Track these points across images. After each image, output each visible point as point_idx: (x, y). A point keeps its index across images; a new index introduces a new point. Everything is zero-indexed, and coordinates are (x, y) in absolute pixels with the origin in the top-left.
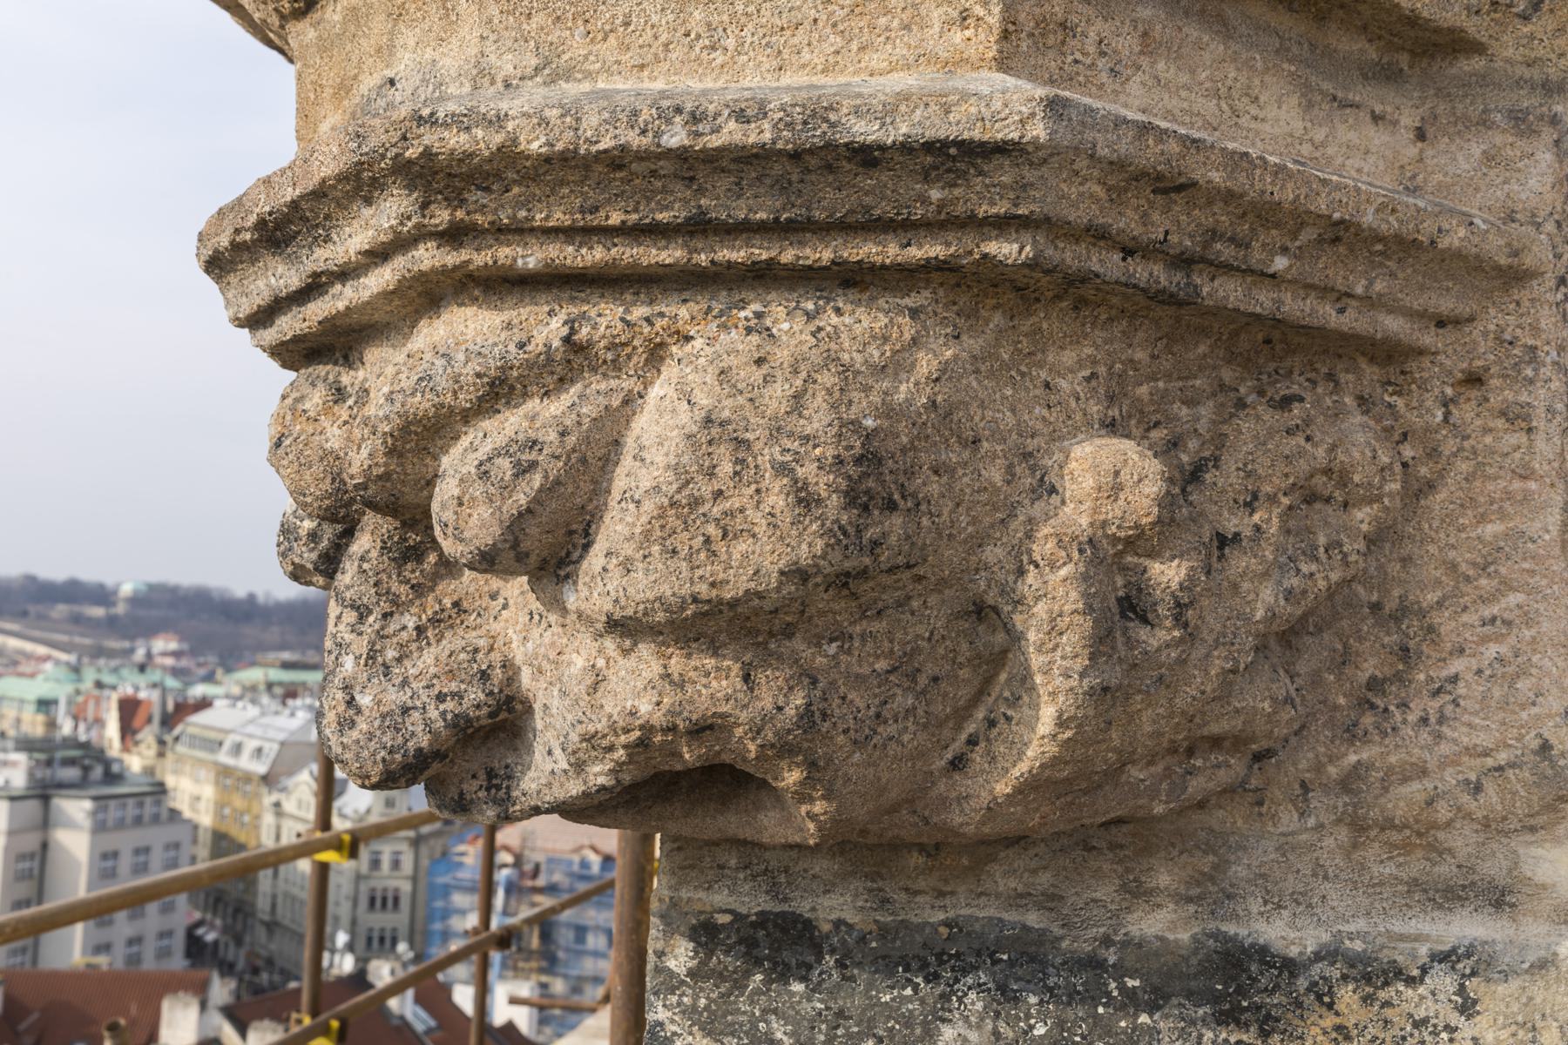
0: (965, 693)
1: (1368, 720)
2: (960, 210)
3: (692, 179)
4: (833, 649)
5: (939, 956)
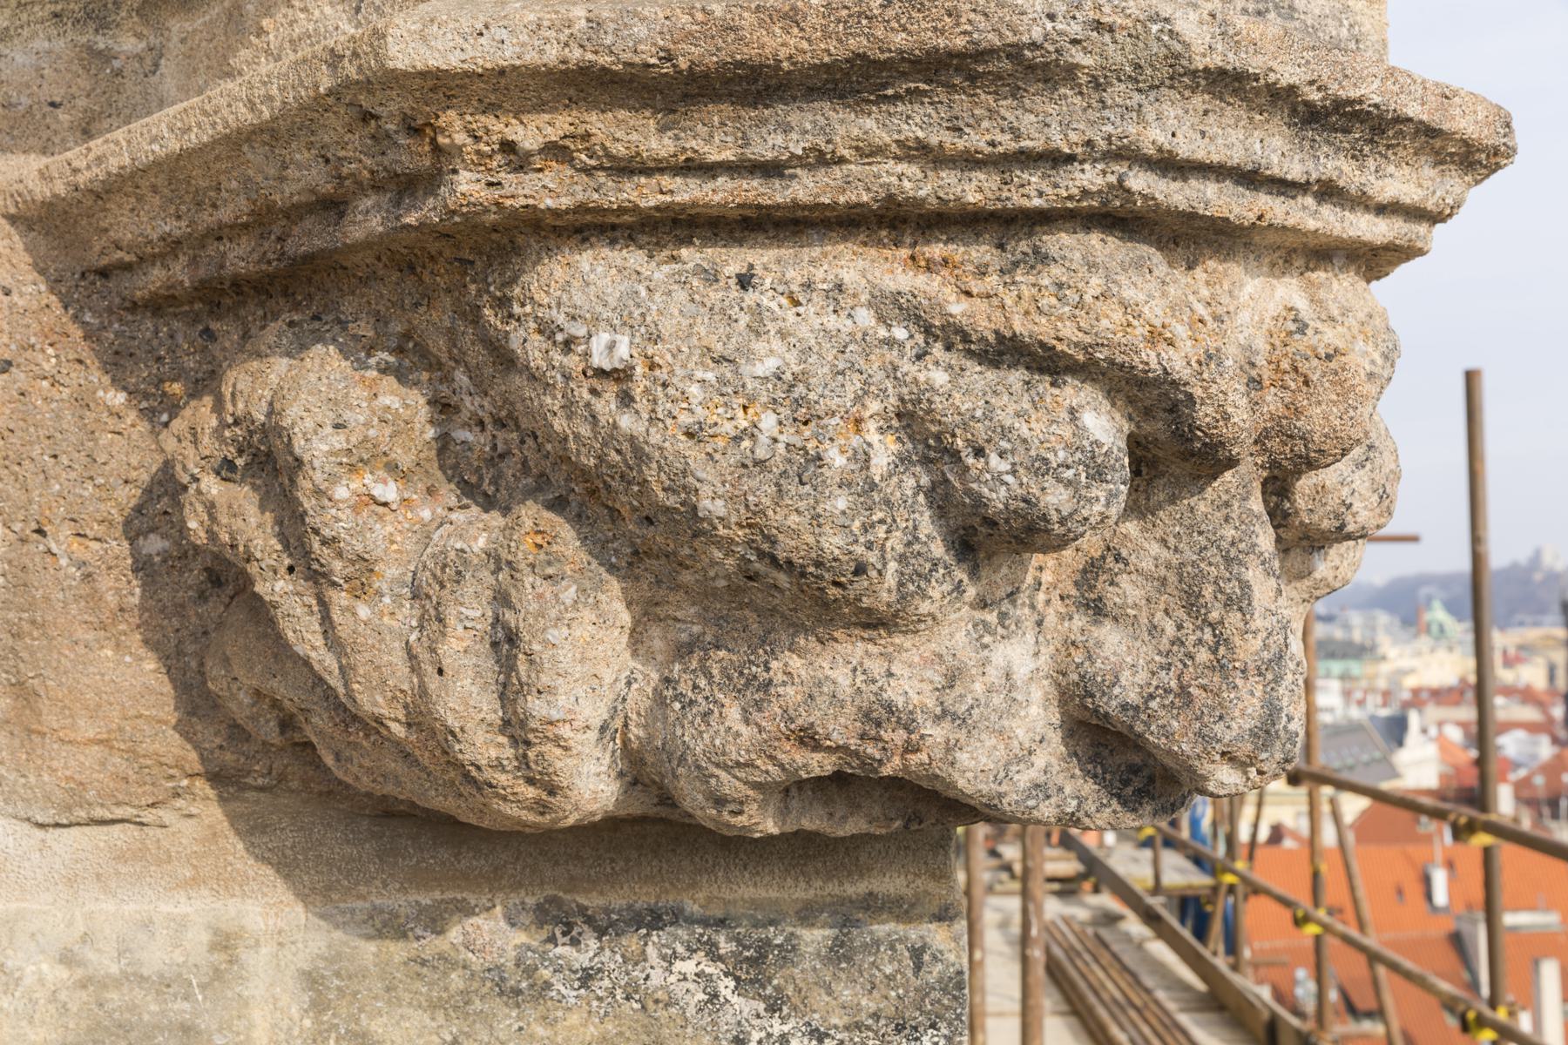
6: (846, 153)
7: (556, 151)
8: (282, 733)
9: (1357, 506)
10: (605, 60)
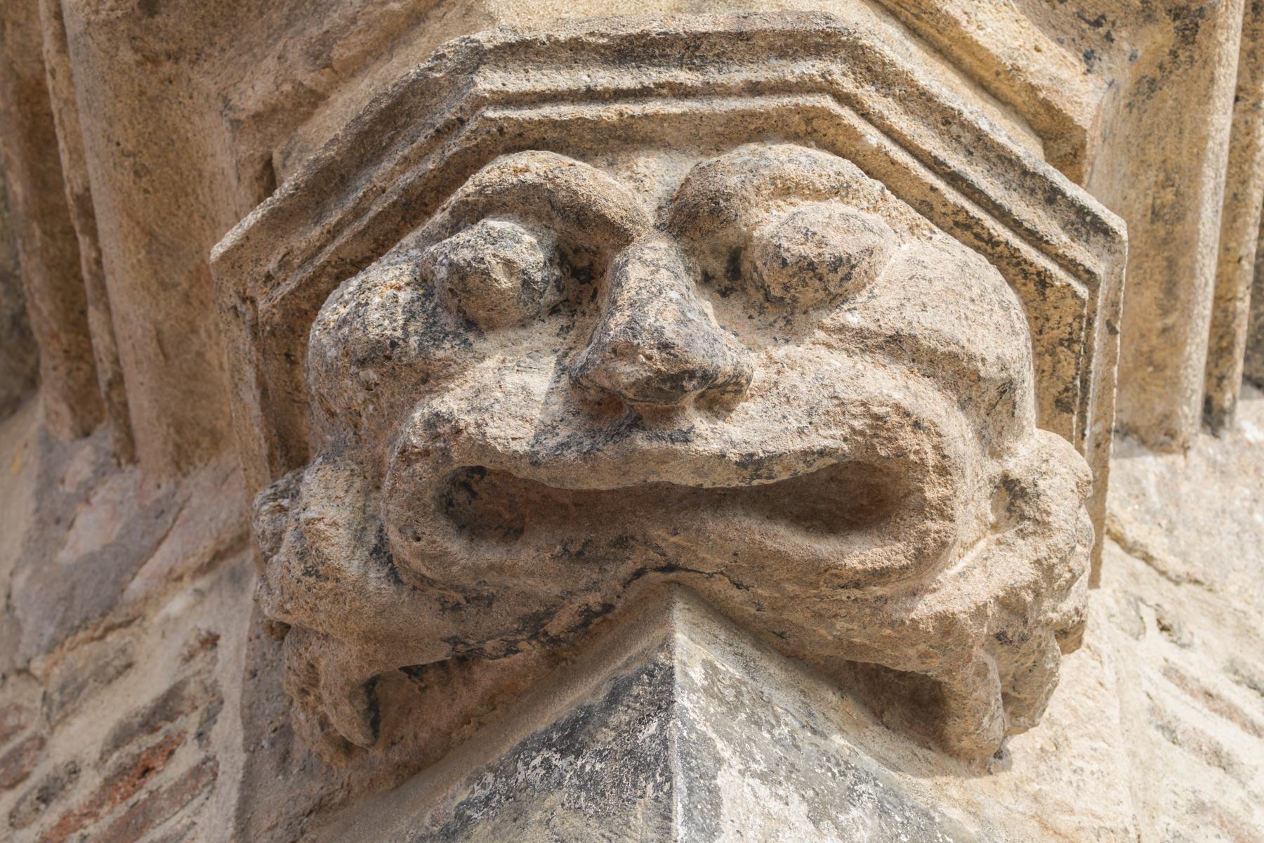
2: (1070, 254)
3: (971, 153)
5: (846, 763)
6: (383, 184)
7: (284, 264)
8: (322, 730)
9: (785, 244)
10: (277, 204)
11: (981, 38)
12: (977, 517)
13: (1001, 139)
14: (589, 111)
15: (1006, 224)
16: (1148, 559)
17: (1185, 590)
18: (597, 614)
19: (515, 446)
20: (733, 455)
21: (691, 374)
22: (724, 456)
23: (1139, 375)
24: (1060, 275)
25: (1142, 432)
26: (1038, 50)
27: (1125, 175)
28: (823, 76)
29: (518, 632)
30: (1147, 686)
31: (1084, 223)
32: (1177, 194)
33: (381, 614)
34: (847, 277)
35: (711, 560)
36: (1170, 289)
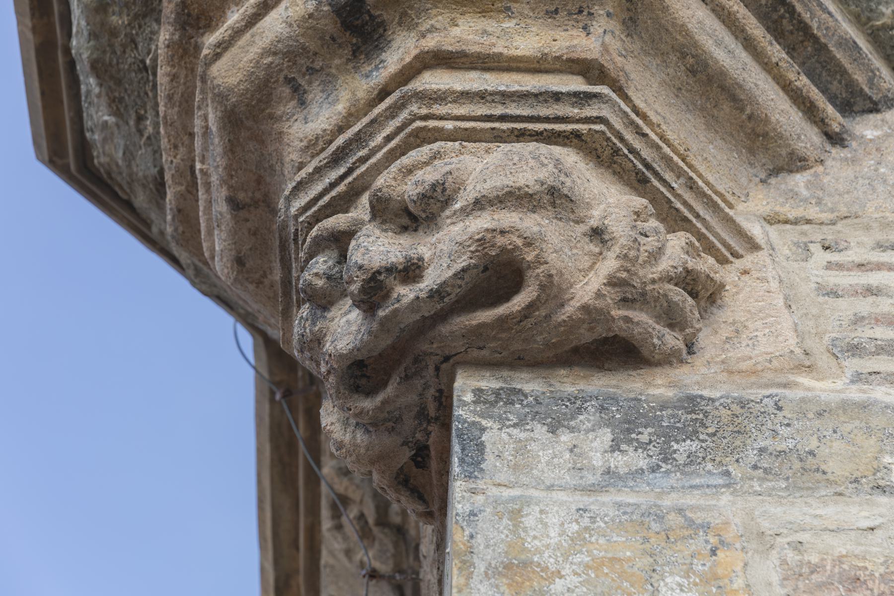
0: (587, 265)
1: (727, 346)
2: (583, 116)
4: (547, 221)
11: (519, 53)
12: (586, 254)
13: (516, 88)
14: (333, 193)
15: (543, 122)
16: (808, 222)
17: (839, 226)
18: (441, 397)
19: (350, 347)
20: (423, 295)
21: (379, 272)
22: (418, 298)
23: (758, 144)
24: (583, 128)
25: (786, 167)
26: (554, 40)
27: (658, 65)
28: (410, 115)
29: (420, 424)
30: (814, 279)
31: (581, 99)
32: (693, 57)
33: (368, 450)
34: (444, 190)
35: (459, 345)
36: (734, 98)
